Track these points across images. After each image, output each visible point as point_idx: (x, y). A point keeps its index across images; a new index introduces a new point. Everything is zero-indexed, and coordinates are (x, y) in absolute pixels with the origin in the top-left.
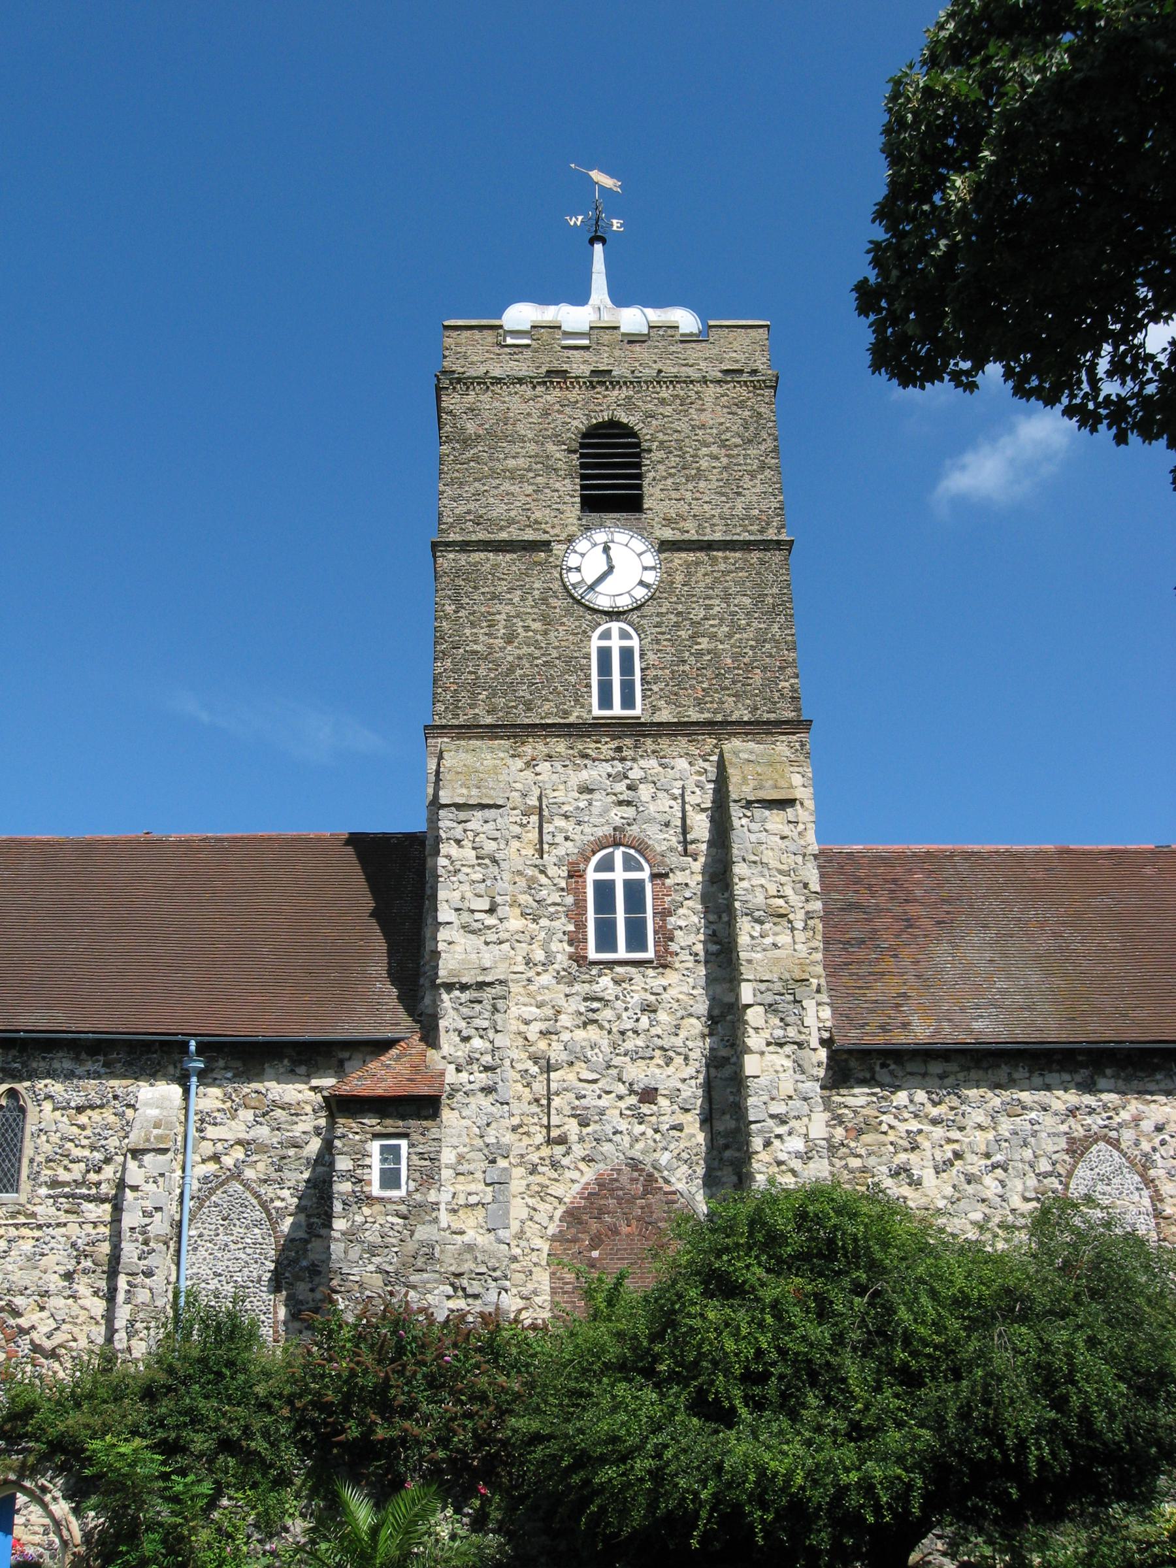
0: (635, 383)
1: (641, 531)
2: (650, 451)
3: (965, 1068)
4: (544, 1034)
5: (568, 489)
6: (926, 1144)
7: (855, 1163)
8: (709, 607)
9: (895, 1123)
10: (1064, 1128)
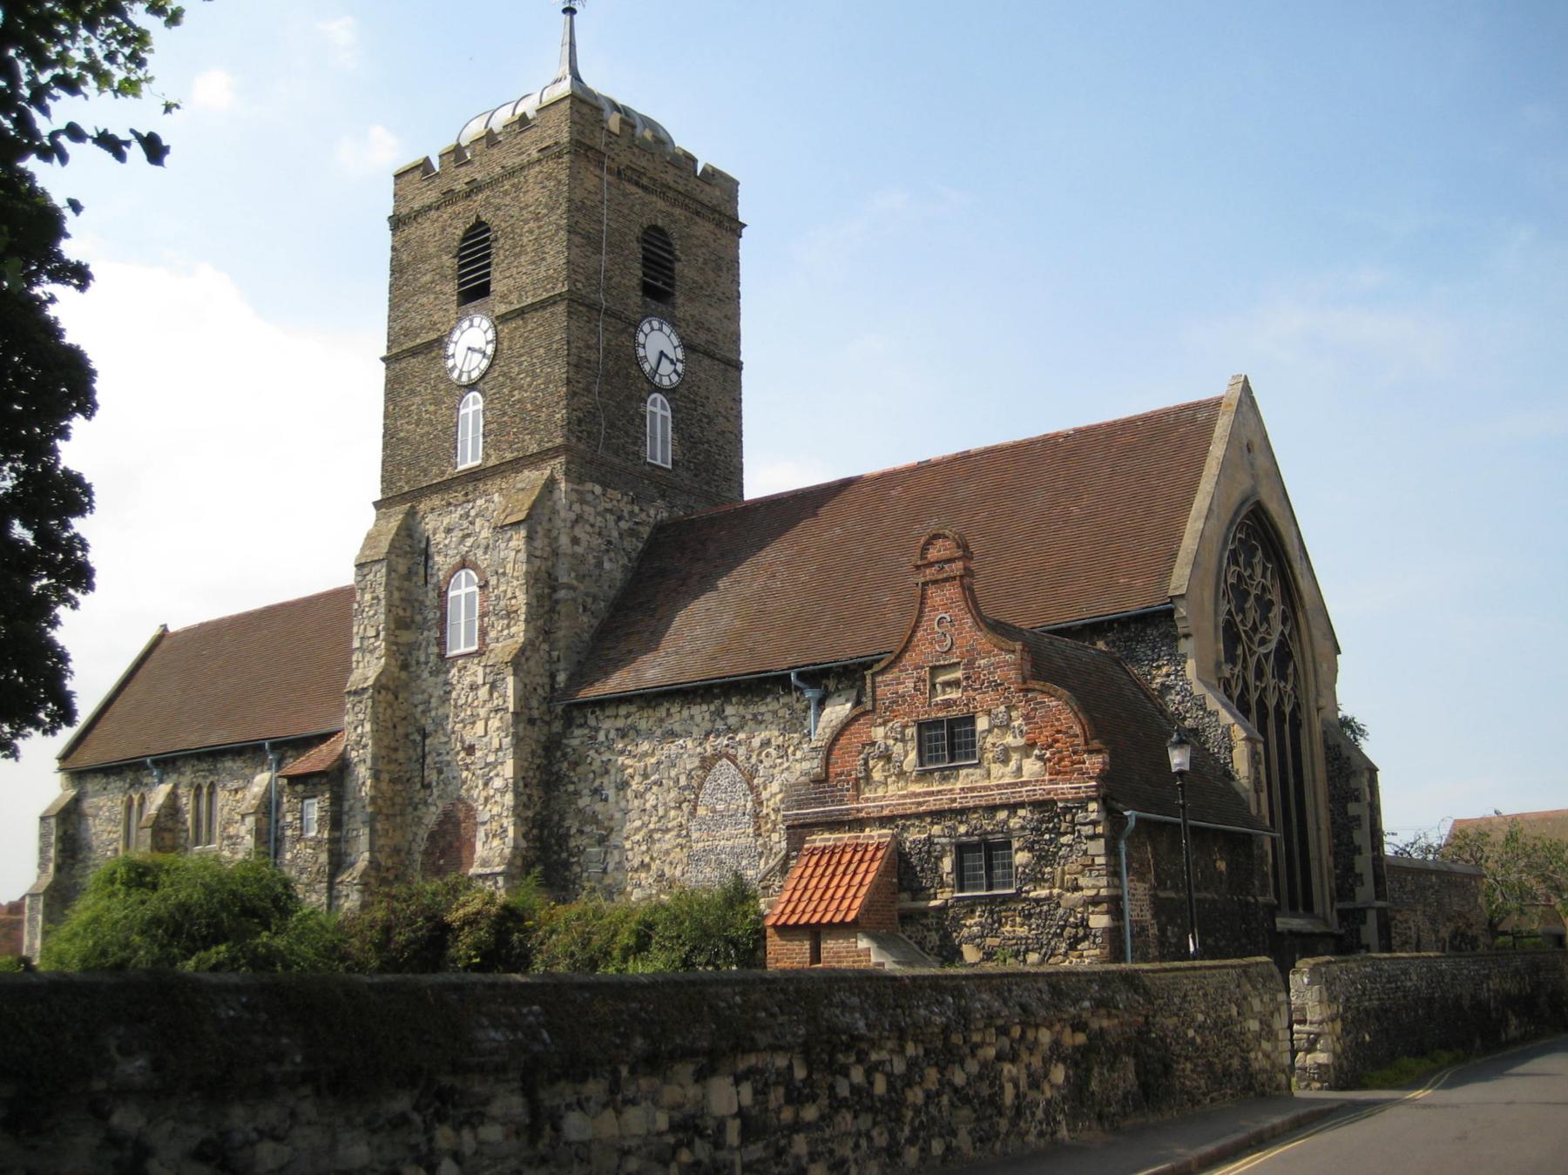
0: (493, 183)
1: (488, 313)
2: (496, 240)
3: (641, 708)
4: (423, 712)
5: (451, 288)
6: (613, 771)
7: (571, 788)
8: (521, 364)
9: (595, 756)
10: (699, 749)
